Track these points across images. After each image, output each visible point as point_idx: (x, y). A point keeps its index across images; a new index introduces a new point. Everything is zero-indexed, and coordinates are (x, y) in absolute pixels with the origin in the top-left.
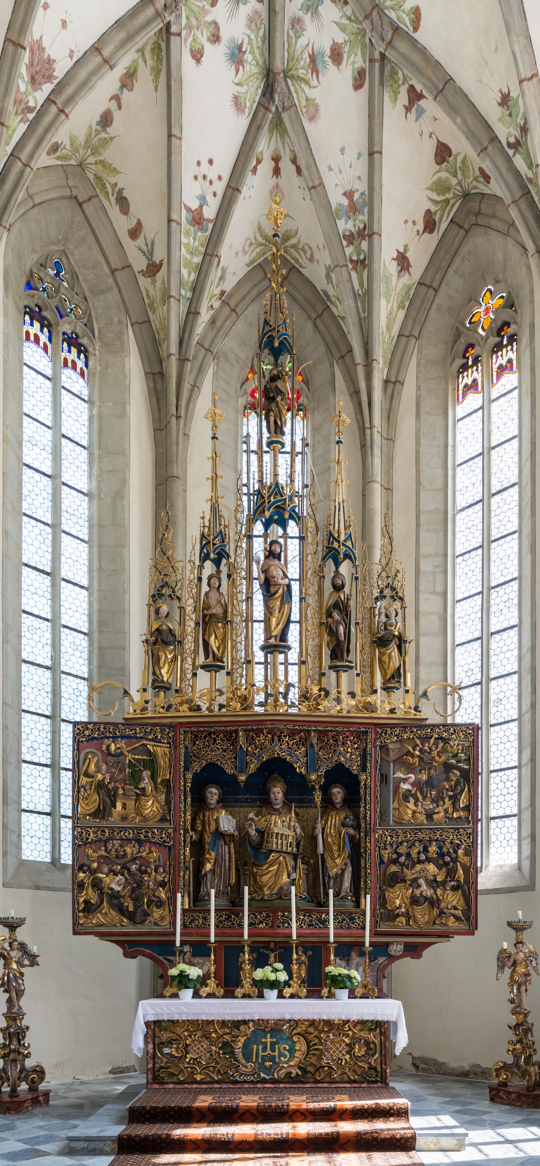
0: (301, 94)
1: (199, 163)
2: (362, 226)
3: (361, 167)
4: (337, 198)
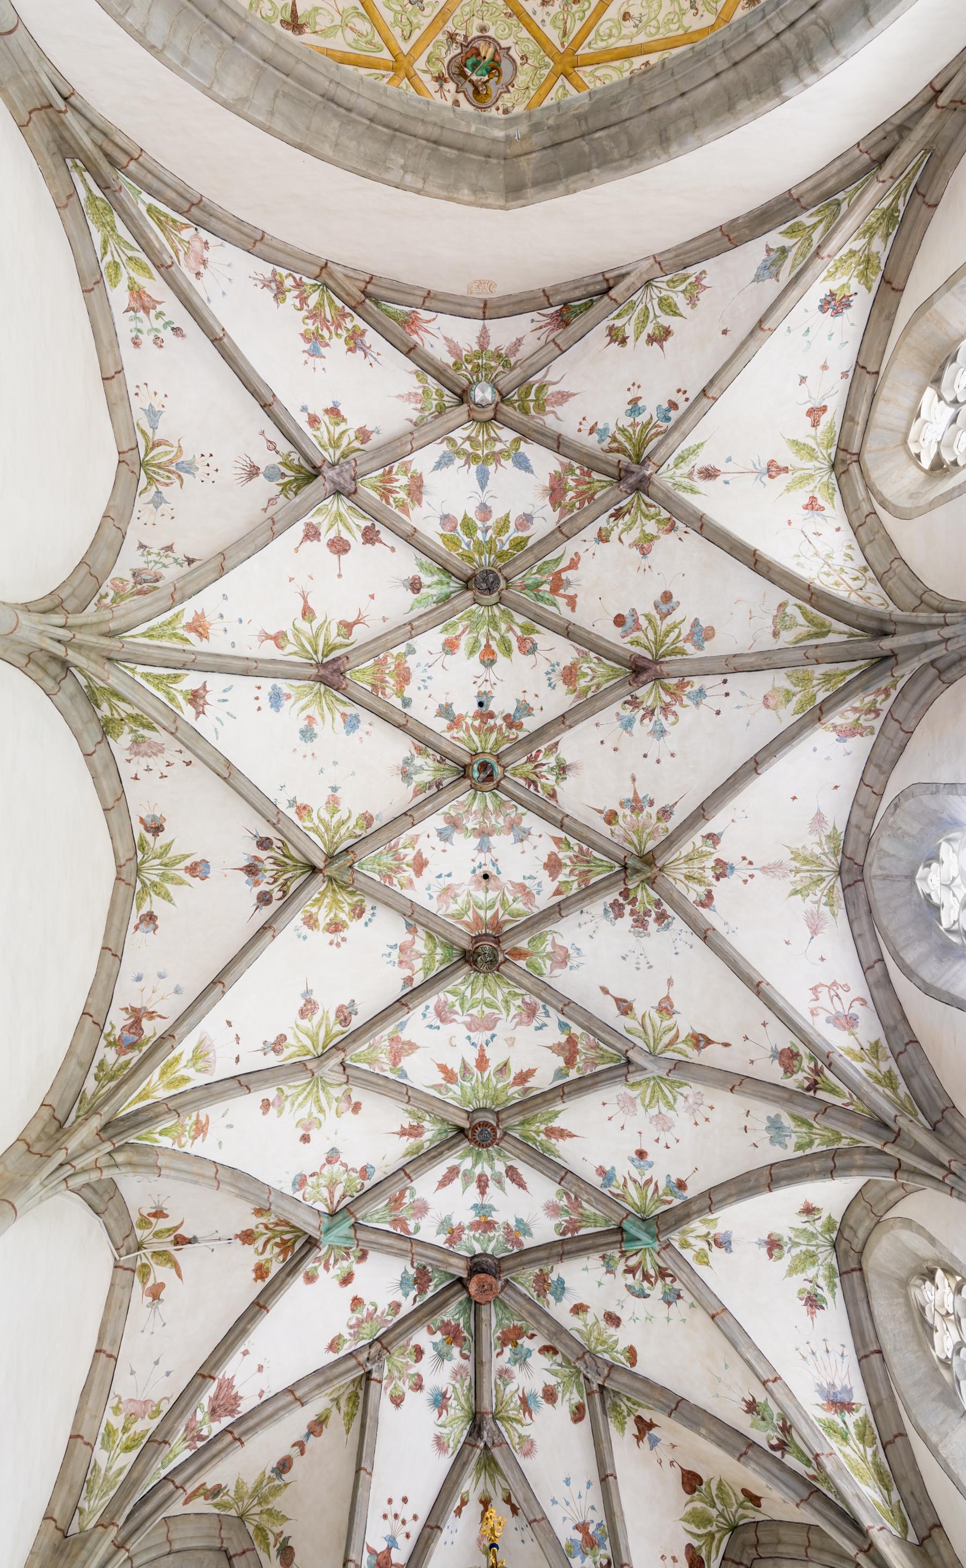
0: (511, 1434)
1: (390, 1501)
2: (605, 1562)
3: (594, 1496)
4: (566, 1533)
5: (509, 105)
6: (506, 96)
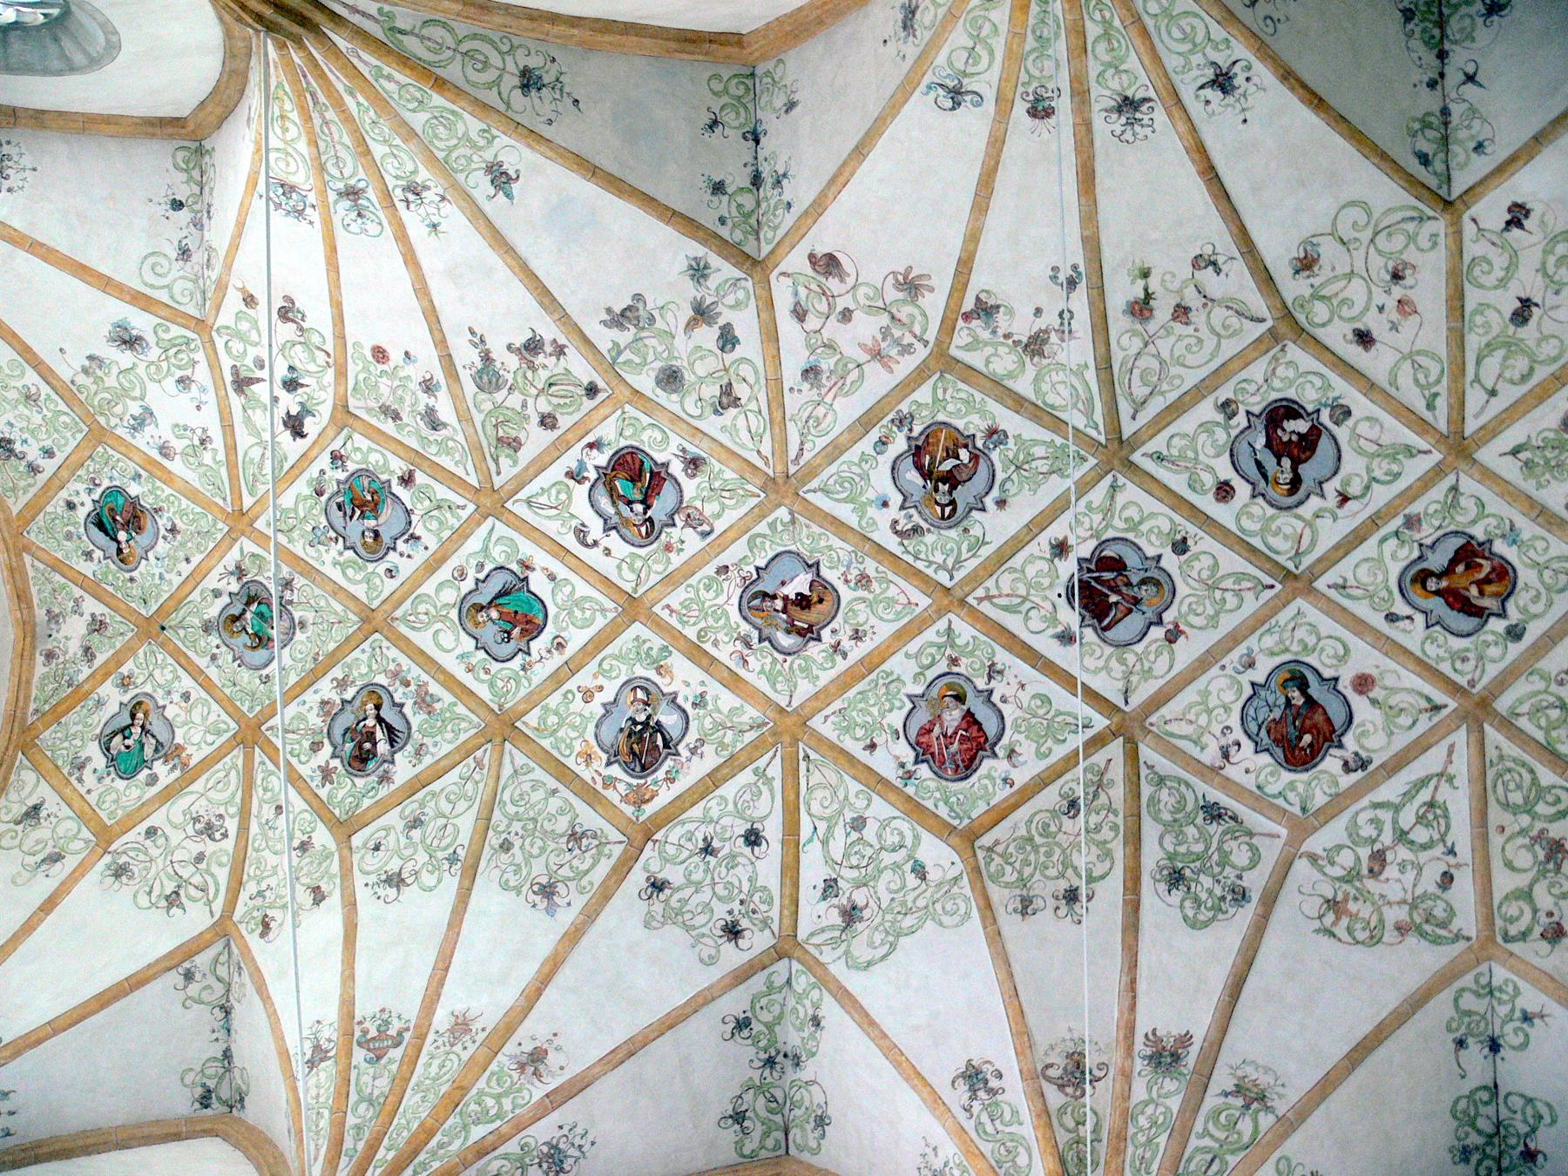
5: (220, 662)
6: (230, 658)
